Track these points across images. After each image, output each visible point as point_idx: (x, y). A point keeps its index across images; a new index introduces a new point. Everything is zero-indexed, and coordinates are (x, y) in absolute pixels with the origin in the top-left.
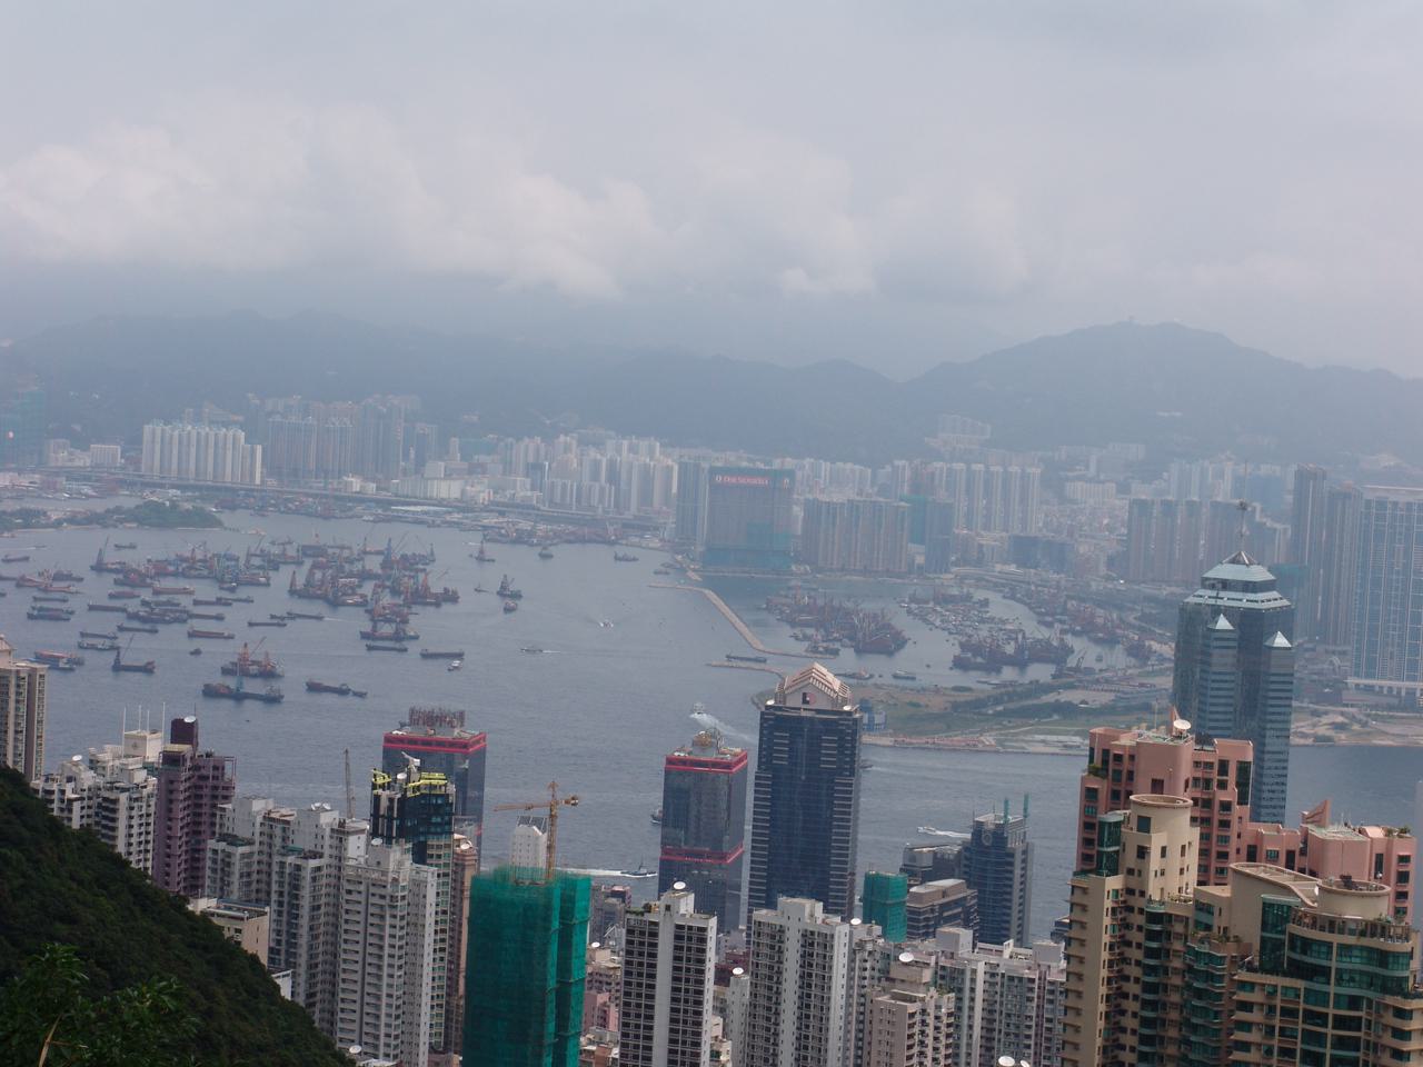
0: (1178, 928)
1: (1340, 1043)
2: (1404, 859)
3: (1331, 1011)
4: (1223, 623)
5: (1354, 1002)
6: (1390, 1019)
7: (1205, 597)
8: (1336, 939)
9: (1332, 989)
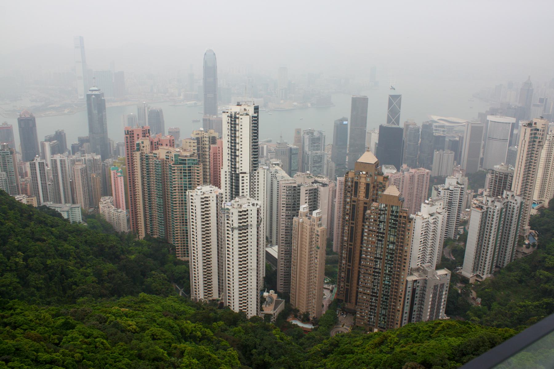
0: (151, 157)
1: (189, 173)
2: (173, 140)
3: (187, 169)
4: (94, 96)
5: (190, 167)
6: (196, 168)
7: (90, 93)
8: (187, 158)
9: (187, 165)
